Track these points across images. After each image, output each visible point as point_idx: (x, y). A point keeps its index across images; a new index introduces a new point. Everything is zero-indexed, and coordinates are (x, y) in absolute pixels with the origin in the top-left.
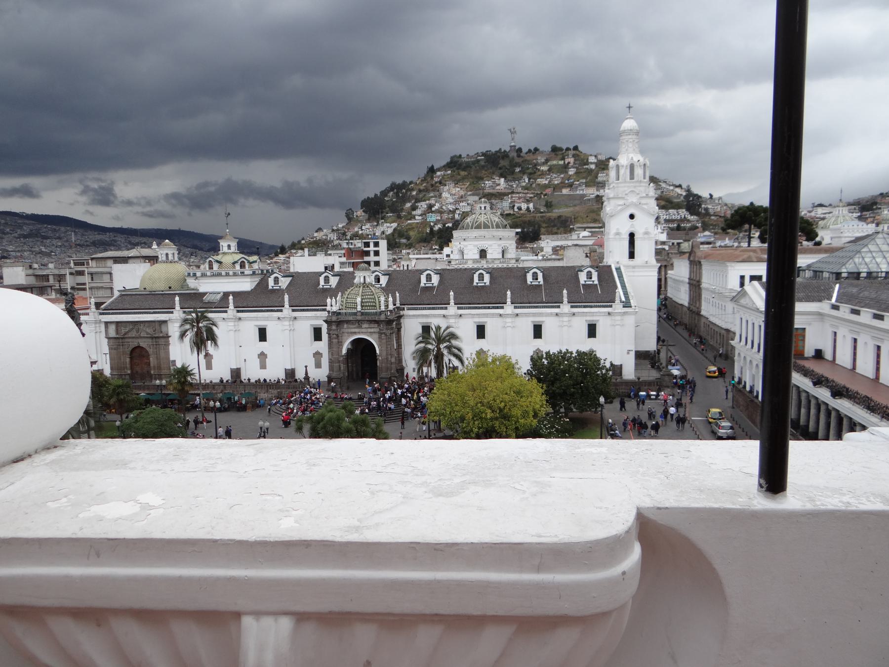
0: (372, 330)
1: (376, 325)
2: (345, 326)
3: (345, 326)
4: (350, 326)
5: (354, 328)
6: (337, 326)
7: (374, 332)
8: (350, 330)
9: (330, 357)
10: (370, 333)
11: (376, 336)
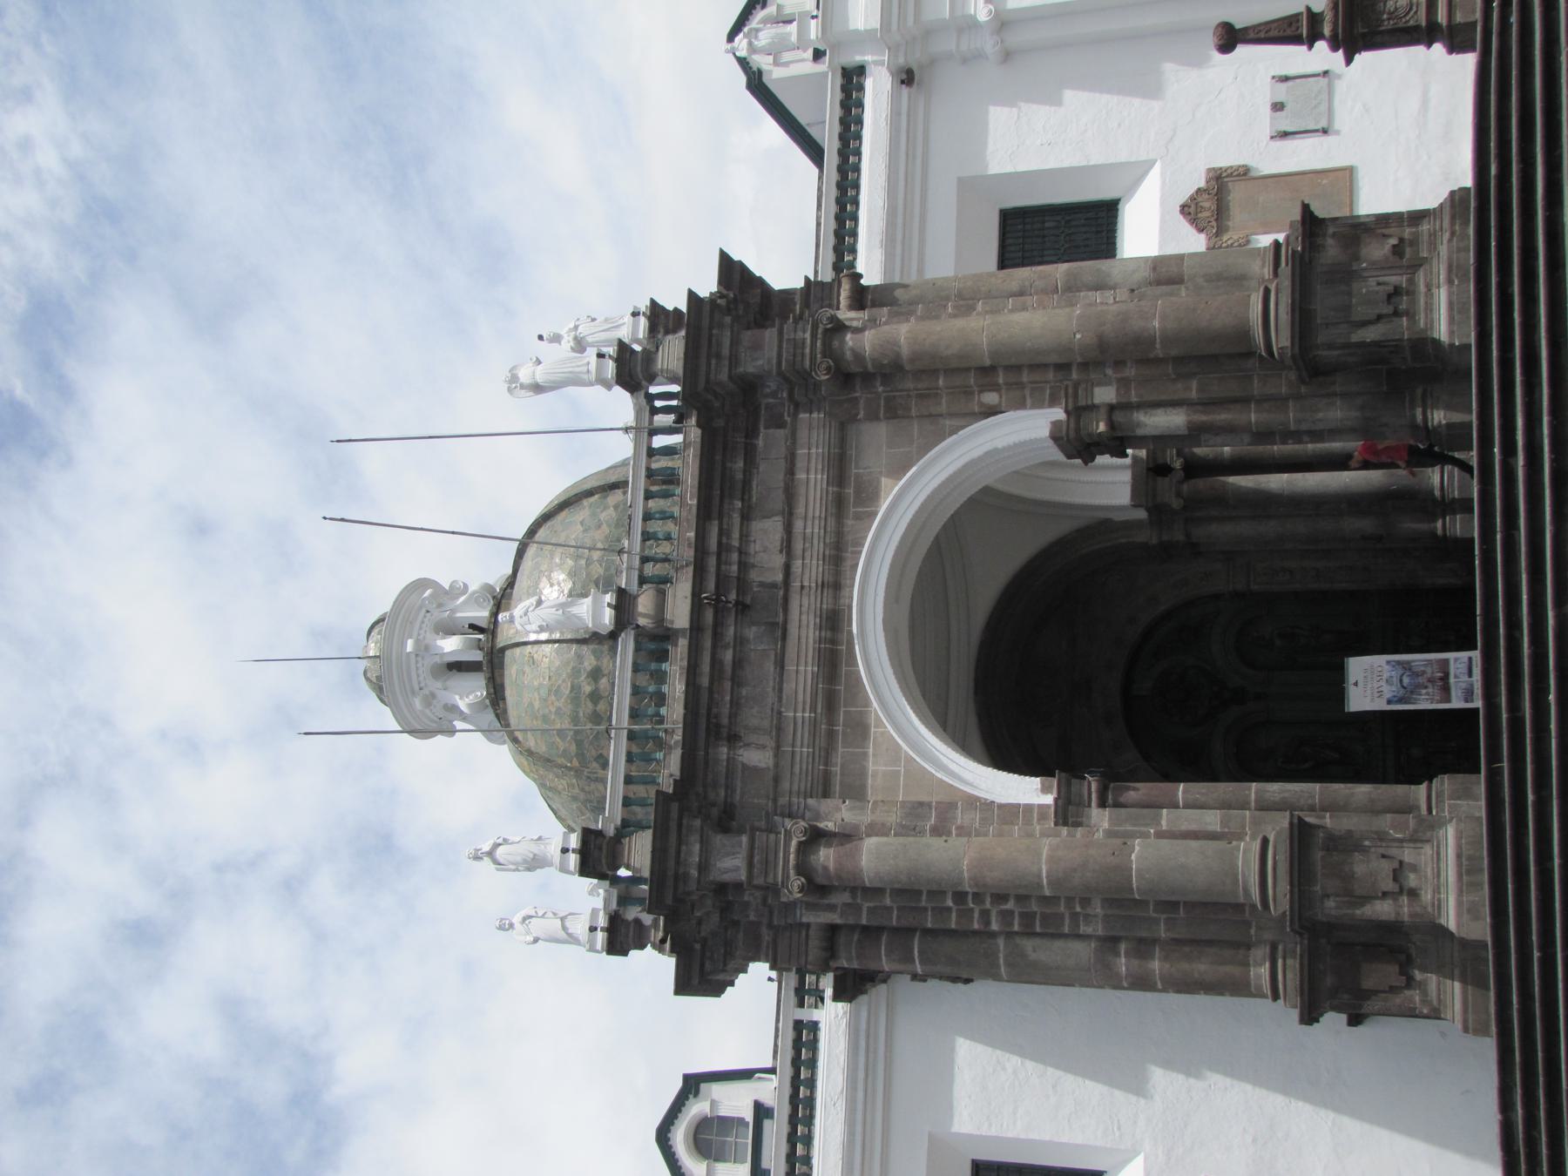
0: (814, 482)
1: (770, 441)
2: (757, 757)
3: (757, 757)
4: (754, 717)
5: (781, 664)
6: (726, 821)
7: (839, 466)
8: (800, 713)
9: (1082, 952)
10: (839, 505)
11: (875, 439)
